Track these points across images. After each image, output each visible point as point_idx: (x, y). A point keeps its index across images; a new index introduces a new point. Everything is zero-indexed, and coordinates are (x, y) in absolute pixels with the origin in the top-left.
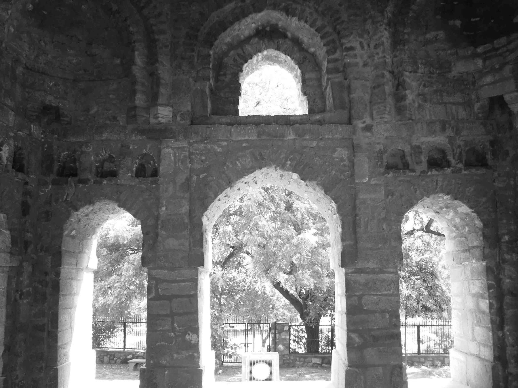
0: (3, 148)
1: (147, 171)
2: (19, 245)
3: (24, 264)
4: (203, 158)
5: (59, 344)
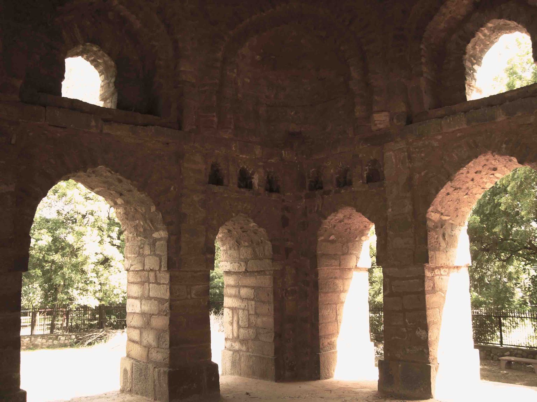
0: (254, 177)
1: (375, 177)
2: (282, 252)
3: (287, 267)
4: (423, 155)
5: (321, 334)
